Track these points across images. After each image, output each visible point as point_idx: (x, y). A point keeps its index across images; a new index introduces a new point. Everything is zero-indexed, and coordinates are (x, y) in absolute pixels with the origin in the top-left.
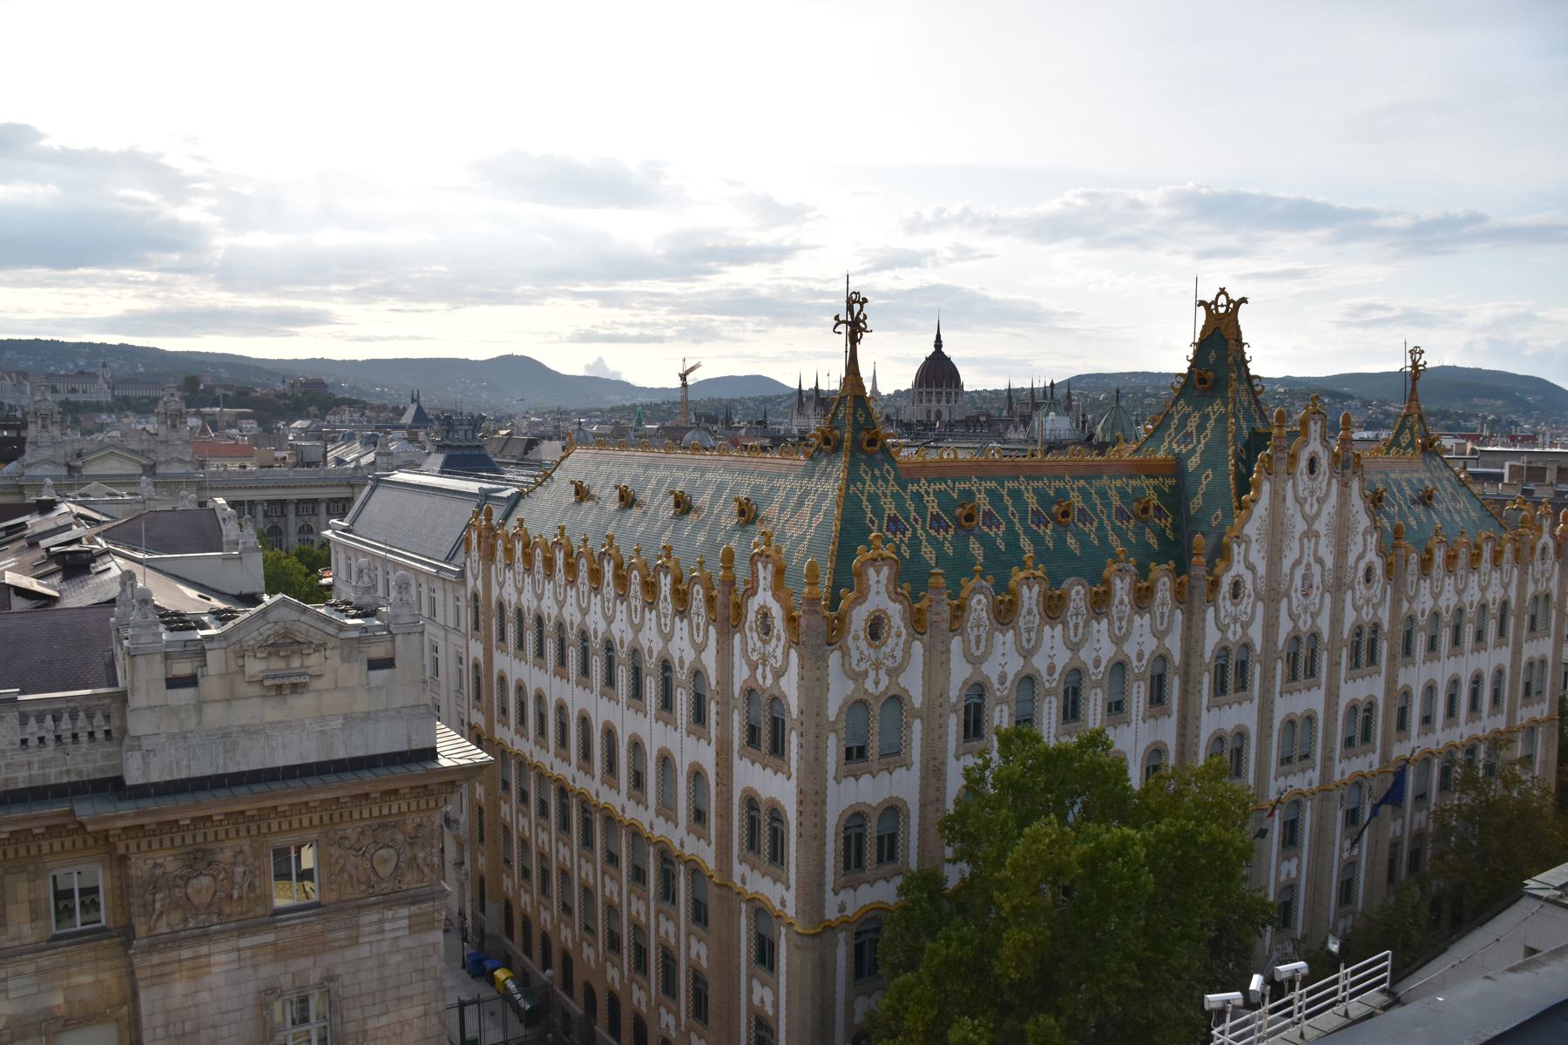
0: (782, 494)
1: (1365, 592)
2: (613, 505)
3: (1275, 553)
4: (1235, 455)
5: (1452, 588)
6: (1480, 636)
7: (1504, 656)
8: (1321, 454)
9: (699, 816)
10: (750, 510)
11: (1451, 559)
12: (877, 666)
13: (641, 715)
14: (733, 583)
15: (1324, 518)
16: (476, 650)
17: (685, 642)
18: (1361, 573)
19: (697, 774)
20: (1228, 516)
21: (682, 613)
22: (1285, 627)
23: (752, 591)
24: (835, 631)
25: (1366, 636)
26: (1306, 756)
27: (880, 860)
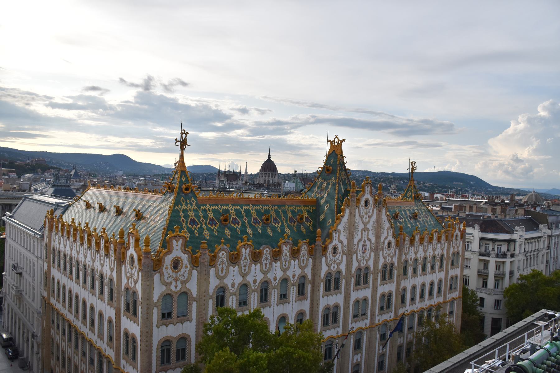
0: (152, 208)
1: (388, 251)
2: (98, 211)
3: (351, 237)
4: (338, 199)
5: (422, 250)
6: (433, 268)
7: (442, 275)
8: (370, 199)
9: (111, 339)
10: (140, 214)
11: (422, 239)
12: (176, 280)
13: (94, 296)
14: (124, 244)
15: (371, 223)
16: (46, 265)
17: (105, 266)
18: (386, 244)
19: (110, 321)
20: (333, 222)
21: (107, 255)
22: (355, 265)
23: (128, 248)
24: (157, 265)
25: (388, 269)
26: (364, 314)
27: (178, 359)
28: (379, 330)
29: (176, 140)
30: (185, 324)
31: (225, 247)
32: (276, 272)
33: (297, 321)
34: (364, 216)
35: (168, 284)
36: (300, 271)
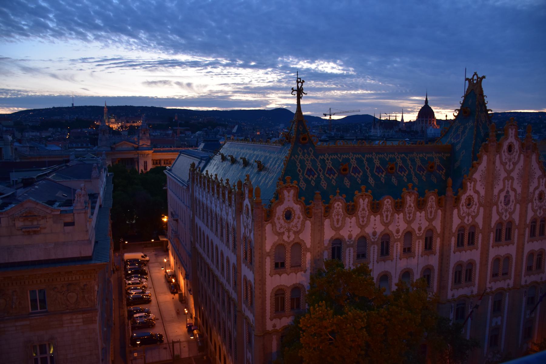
1: (538, 204)
8: (515, 143)
12: (289, 230)
15: (516, 171)
18: (536, 195)
22: (495, 218)
24: (269, 215)
26: (506, 274)
28: (525, 292)
29: (292, 89)
30: (299, 274)
31: (341, 197)
32: (399, 224)
33: (424, 276)
34: (506, 163)
35: (281, 234)
36: (427, 223)
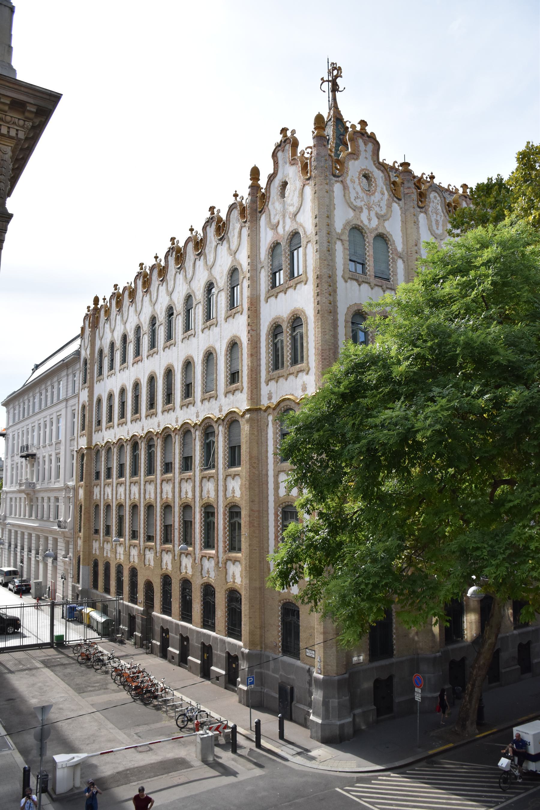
29: (322, 79)
